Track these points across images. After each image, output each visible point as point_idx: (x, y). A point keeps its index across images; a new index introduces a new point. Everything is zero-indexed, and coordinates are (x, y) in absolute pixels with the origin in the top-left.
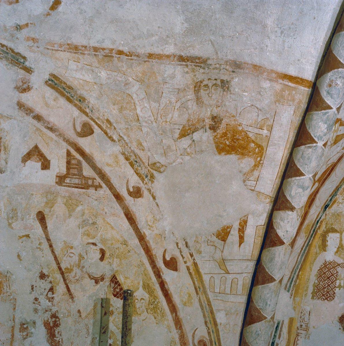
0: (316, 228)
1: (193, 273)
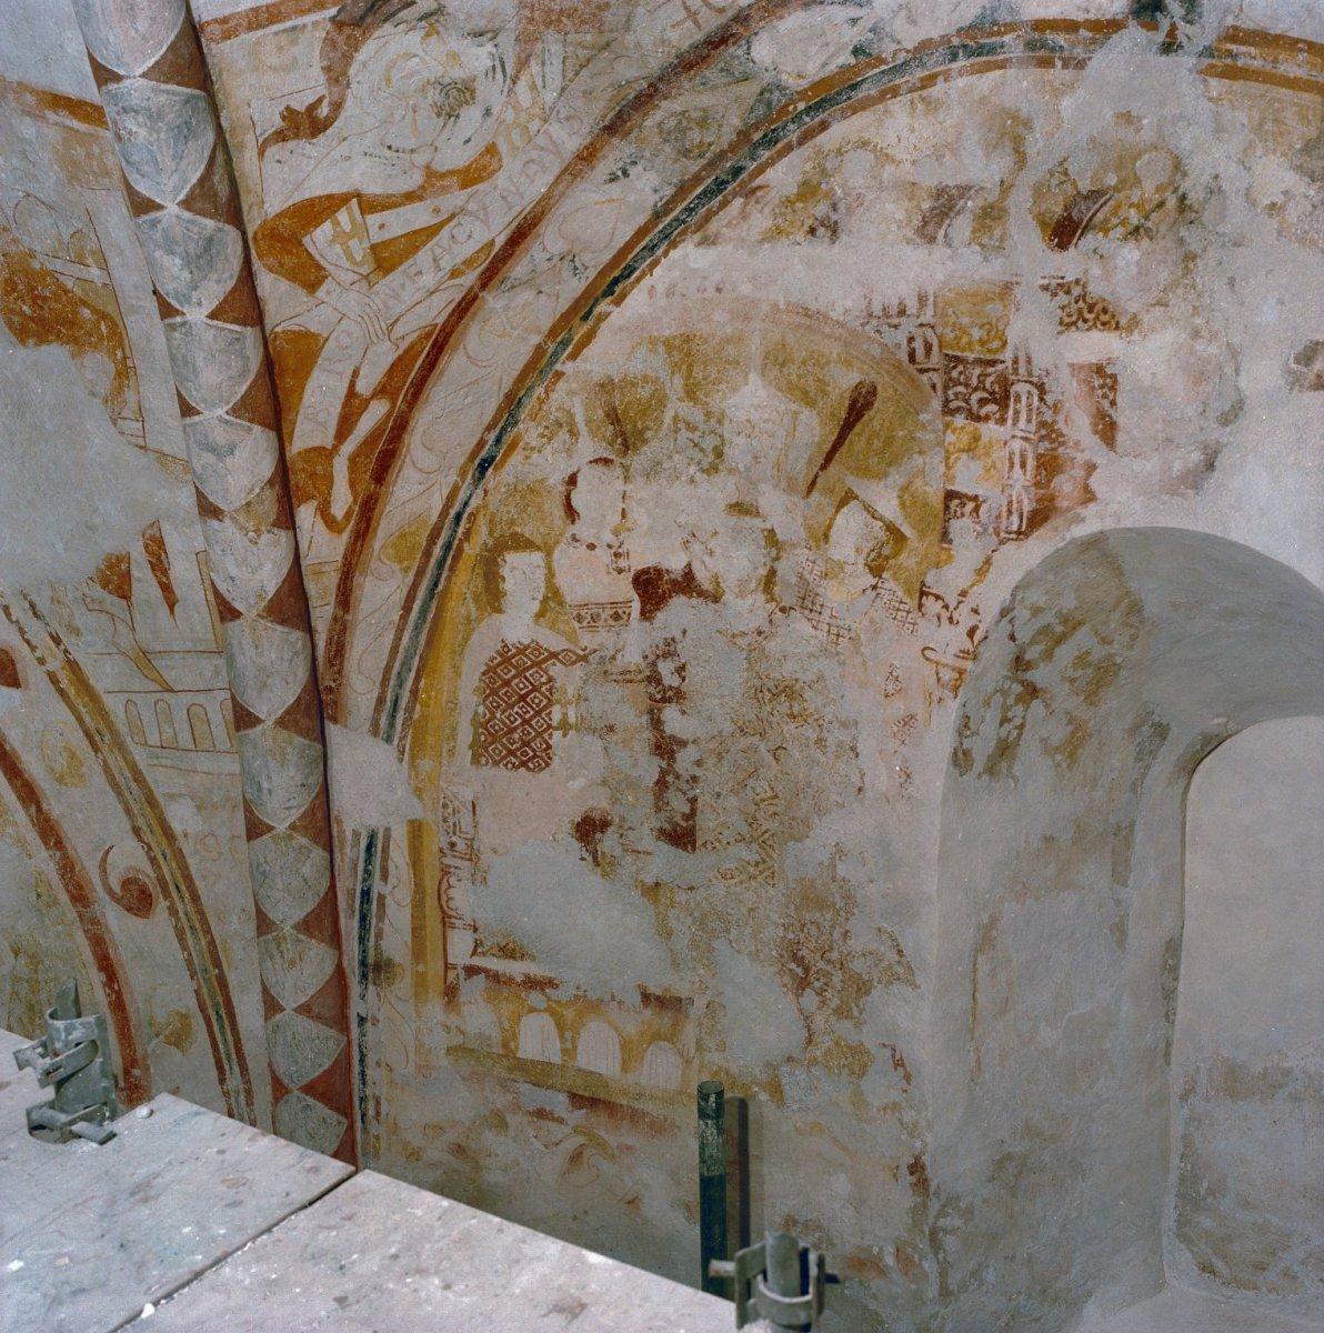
0: (453, 536)
1: (72, 692)
